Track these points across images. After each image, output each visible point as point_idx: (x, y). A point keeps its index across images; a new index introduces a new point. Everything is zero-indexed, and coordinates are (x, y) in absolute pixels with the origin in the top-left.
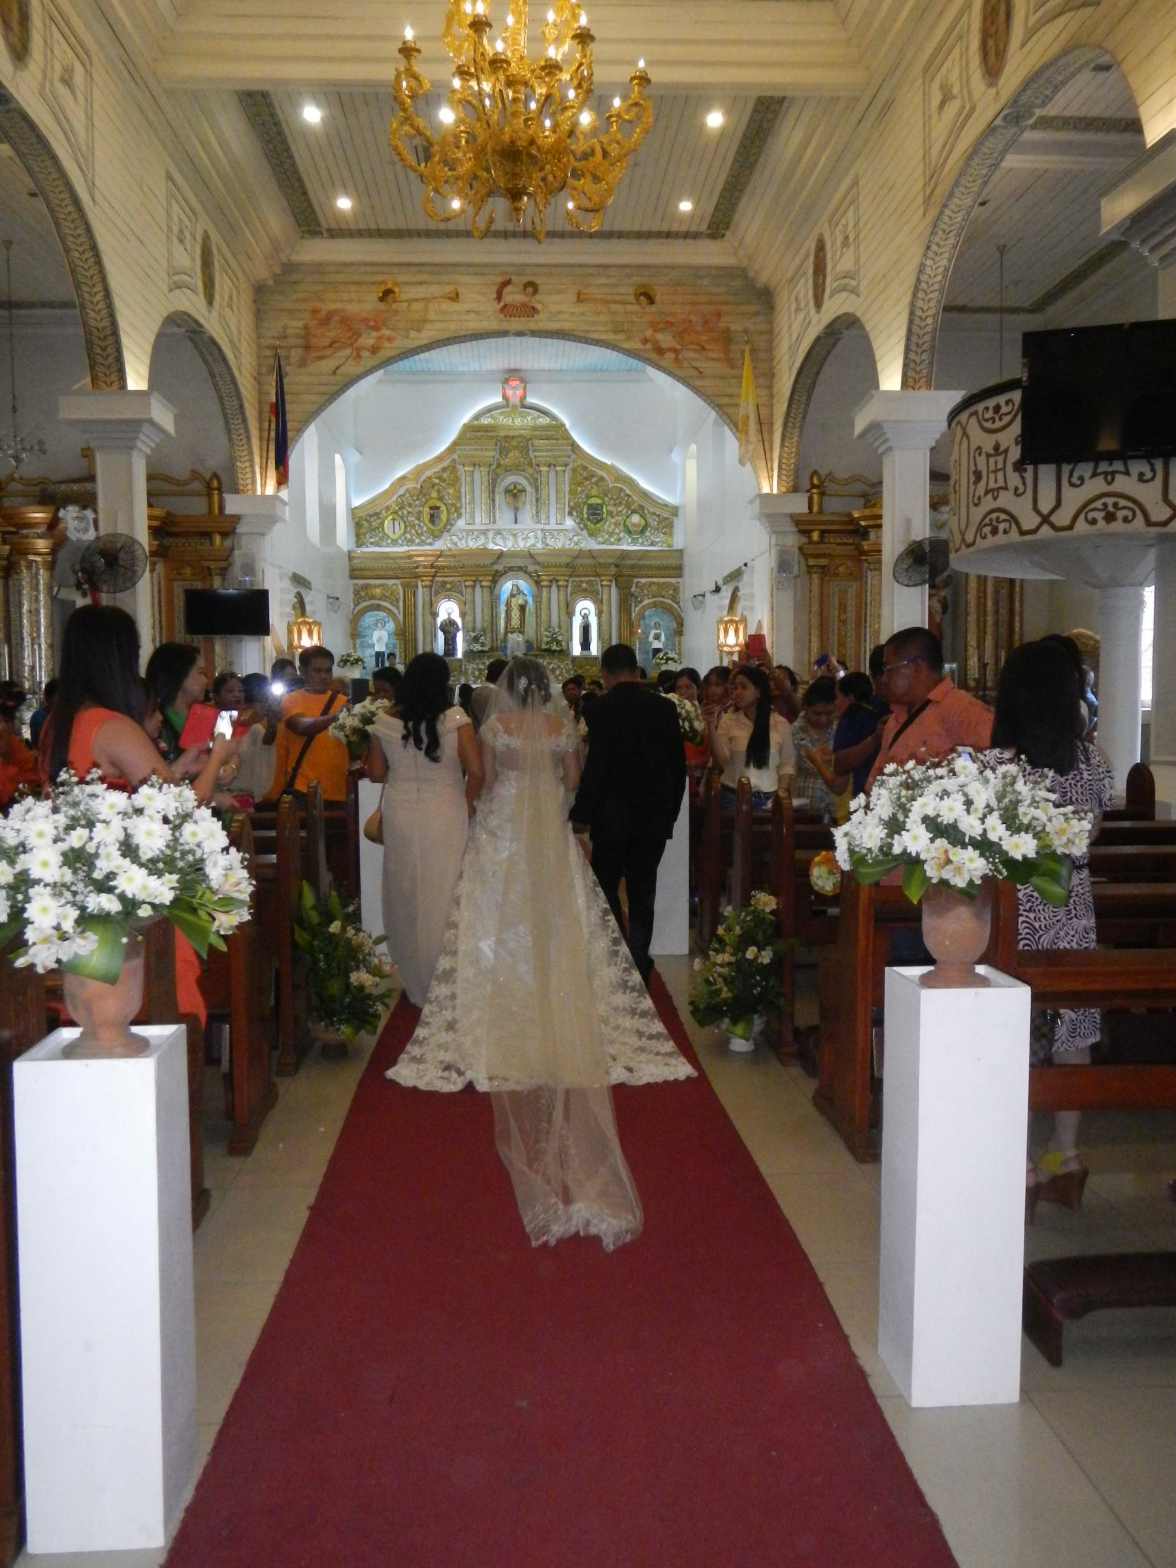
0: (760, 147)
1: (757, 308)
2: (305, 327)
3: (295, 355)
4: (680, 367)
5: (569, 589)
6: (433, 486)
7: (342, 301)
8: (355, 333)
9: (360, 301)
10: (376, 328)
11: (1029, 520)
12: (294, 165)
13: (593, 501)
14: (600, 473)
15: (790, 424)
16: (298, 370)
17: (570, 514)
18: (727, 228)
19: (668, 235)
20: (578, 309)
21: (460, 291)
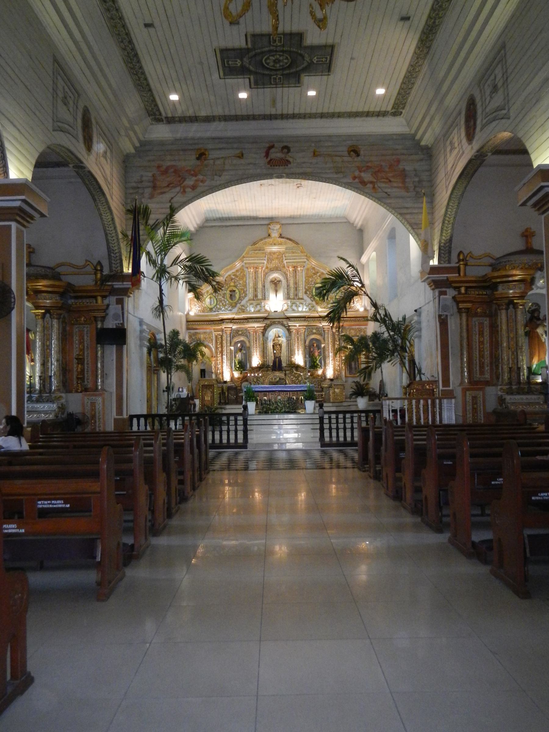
0: (432, 40)
1: (422, 156)
2: (153, 176)
3: (148, 191)
4: (376, 192)
5: (306, 333)
6: (232, 279)
7: (175, 160)
8: (182, 178)
9: (185, 160)
10: (196, 176)
12: (141, 67)
14: (322, 271)
15: (446, 222)
16: (149, 200)
17: (306, 293)
18: (403, 108)
19: (369, 114)
20: (314, 160)
21: (244, 152)
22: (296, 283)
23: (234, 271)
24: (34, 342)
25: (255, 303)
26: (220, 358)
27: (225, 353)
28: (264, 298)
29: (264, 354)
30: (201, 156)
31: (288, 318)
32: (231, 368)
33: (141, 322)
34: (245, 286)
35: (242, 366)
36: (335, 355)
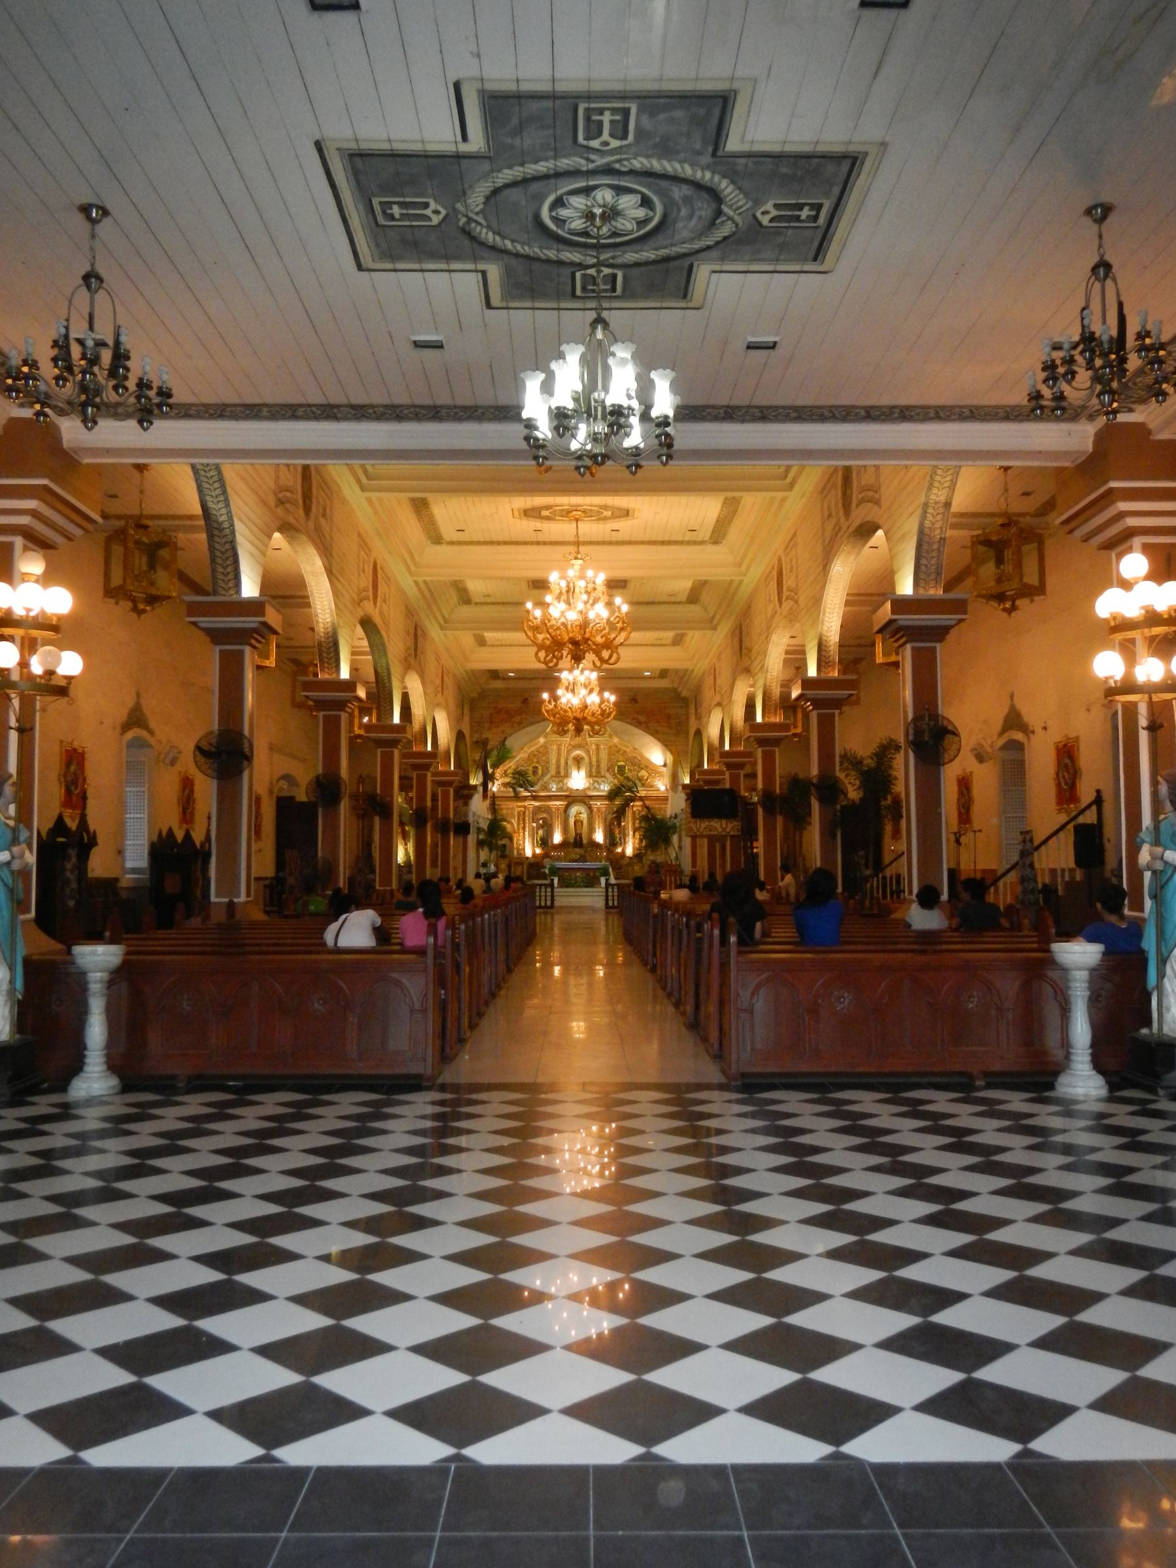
3: (487, 725)
10: (521, 714)
11: (695, 830)
13: (620, 764)
17: (608, 771)
22: (598, 761)
23: (537, 746)
24: (409, 832)
25: (557, 779)
26: (521, 834)
27: (527, 829)
28: (567, 775)
29: (565, 830)
30: (525, 701)
31: (591, 797)
32: (533, 844)
33: (474, 814)
34: (548, 762)
35: (545, 842)
36: (634, 833)
